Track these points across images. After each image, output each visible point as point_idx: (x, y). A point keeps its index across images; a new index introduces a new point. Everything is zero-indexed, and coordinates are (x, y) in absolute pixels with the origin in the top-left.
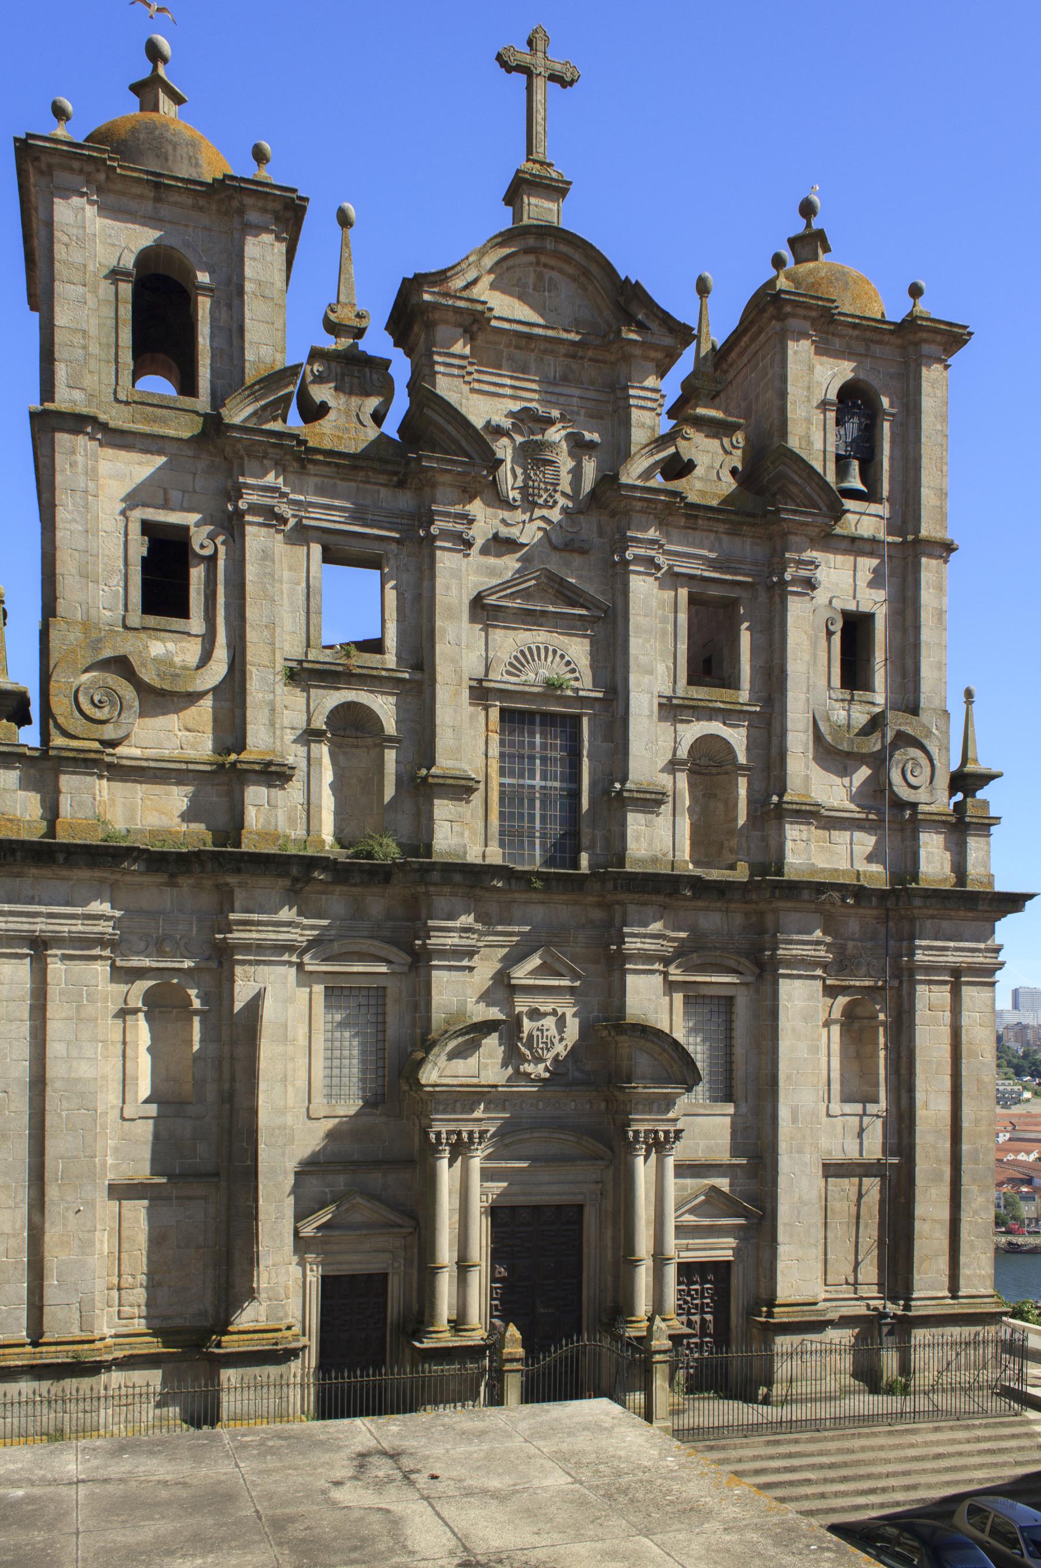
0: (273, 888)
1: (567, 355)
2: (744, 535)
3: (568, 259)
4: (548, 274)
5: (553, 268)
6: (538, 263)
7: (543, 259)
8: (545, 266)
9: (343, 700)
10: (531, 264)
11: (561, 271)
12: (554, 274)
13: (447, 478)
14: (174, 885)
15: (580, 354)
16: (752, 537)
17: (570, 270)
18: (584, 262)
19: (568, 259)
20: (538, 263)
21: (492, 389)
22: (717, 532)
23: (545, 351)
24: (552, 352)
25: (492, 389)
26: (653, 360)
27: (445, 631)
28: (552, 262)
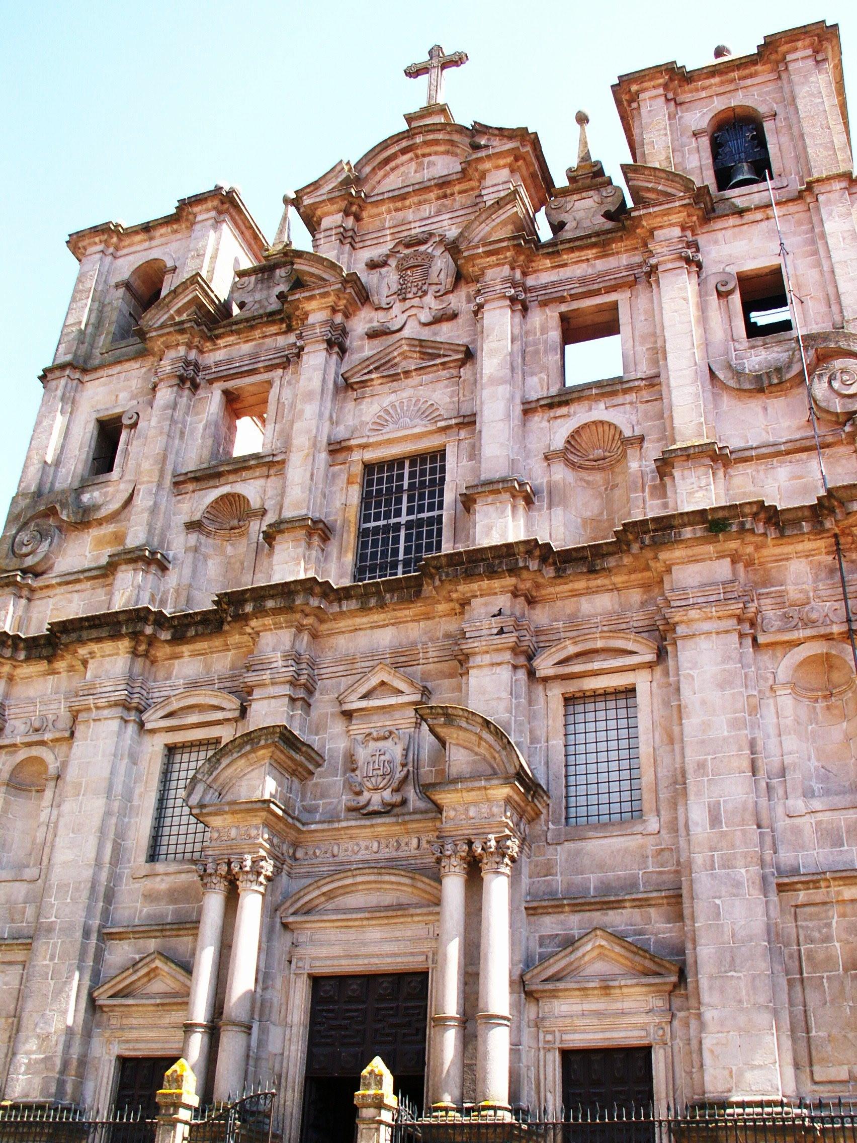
0: (117, 654)
1: (438, 198)
2: (618, 253)
3: (436, 142)
4: (426, 160)
5: (429, 155)
6: (417, 157)
7: (419, 152)
8: (424, 156)
9: (219, 494)
10: (412, 159)
11: (436, 153)
12: (432, 158)
13: (314, 305)
14: (54, 672)
15: (449, 192)
16: (626, 251)
17: (441, 148)
18: (447, 137)
19: (436, 142)
20: (417, 157)
21: (375, 242)
22: (588, 260)
23: (420, 203)
24: (425, 201)
25: (375, 242)
26: (504, 166)
27: (302, 412)
28: (427, 150)
